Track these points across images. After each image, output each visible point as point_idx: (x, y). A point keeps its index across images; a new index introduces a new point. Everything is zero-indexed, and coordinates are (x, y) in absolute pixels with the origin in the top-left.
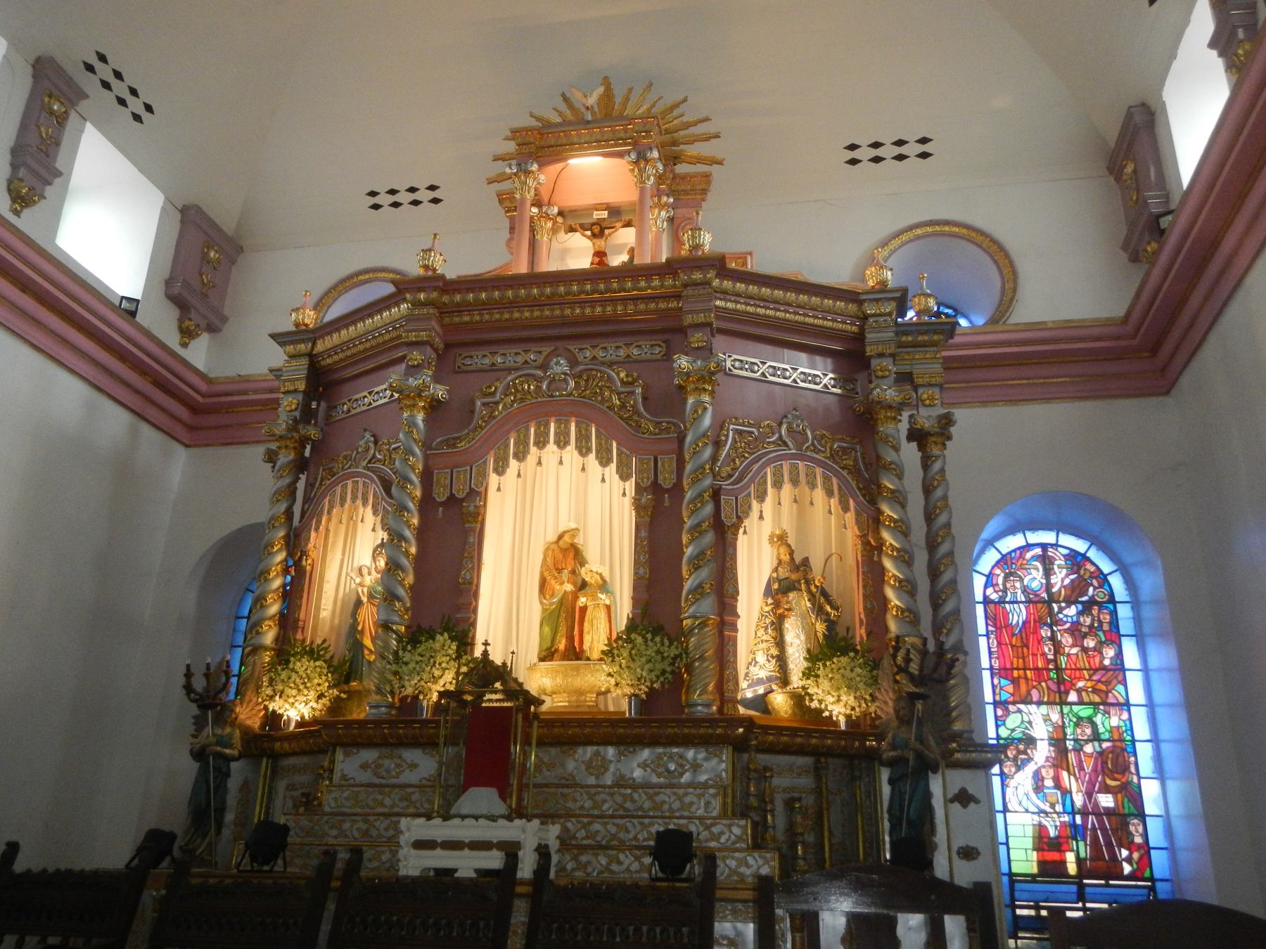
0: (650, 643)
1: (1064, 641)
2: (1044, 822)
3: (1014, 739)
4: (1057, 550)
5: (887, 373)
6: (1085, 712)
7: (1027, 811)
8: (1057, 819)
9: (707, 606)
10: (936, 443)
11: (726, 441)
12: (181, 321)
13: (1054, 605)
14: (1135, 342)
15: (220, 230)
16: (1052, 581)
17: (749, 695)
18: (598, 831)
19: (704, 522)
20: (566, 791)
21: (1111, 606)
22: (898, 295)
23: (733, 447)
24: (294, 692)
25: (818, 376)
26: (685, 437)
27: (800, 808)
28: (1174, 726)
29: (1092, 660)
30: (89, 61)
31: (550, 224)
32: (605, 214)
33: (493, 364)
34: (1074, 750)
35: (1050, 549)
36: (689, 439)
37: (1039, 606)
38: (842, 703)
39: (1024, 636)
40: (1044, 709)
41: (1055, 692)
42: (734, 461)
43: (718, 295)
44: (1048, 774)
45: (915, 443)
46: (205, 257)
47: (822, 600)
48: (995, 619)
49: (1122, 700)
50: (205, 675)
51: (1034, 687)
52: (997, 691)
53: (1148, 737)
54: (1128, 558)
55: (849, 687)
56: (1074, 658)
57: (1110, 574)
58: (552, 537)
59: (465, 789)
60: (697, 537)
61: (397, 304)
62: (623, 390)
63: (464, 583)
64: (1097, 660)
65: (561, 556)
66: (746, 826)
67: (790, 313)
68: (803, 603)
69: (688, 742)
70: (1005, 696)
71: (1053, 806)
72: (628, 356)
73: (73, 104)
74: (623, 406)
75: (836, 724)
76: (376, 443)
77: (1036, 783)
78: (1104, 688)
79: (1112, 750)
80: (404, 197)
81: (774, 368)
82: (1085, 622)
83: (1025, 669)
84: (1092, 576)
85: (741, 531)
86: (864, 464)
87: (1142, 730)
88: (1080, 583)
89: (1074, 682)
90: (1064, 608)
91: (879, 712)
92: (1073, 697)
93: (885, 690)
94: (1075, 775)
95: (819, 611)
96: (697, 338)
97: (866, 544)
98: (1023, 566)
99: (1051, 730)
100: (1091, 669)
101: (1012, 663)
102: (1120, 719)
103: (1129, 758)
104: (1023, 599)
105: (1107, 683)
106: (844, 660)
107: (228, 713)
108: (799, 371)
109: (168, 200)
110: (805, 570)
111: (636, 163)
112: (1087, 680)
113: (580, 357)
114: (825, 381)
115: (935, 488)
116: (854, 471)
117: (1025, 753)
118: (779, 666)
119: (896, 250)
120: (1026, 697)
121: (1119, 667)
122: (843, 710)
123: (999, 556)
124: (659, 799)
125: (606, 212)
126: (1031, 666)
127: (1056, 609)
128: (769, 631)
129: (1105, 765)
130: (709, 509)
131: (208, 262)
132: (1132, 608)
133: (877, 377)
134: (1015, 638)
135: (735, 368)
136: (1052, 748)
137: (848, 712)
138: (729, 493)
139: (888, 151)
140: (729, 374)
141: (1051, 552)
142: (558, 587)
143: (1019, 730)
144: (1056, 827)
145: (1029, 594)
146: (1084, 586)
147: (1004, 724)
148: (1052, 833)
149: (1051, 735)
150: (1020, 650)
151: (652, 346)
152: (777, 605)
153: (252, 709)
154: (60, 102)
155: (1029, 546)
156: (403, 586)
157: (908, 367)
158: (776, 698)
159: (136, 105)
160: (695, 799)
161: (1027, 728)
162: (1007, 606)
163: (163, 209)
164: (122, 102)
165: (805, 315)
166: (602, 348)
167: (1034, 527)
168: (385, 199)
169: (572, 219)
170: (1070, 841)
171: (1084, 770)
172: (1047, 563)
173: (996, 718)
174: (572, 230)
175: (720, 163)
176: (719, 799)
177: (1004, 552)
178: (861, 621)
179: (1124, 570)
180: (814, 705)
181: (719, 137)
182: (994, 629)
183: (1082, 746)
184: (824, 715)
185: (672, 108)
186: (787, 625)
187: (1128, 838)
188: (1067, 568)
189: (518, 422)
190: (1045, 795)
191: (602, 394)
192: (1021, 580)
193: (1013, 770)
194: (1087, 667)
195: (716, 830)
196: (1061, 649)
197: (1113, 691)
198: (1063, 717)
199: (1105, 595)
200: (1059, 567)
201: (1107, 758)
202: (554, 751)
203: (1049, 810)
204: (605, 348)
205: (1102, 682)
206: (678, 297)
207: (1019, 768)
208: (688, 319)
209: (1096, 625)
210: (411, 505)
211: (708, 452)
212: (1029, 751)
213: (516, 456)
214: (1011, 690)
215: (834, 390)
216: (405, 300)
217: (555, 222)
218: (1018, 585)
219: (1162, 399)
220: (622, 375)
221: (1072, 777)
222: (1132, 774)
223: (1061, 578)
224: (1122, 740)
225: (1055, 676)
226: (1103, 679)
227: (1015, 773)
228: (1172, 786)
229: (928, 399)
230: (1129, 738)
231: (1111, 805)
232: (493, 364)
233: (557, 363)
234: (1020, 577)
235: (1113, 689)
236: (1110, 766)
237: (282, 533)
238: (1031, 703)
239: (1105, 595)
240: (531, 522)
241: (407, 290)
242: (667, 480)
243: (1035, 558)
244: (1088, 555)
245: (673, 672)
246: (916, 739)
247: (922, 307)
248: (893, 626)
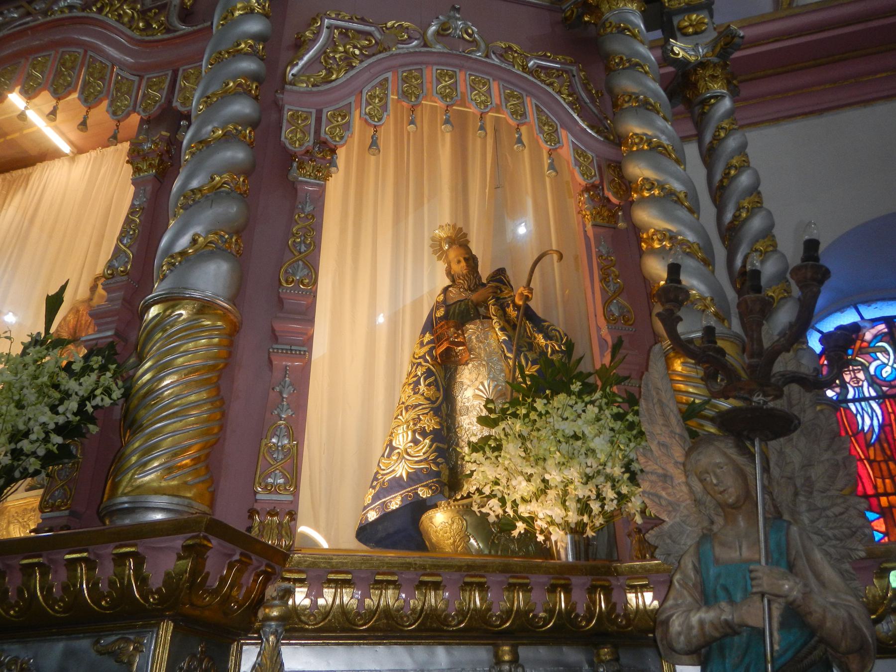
11: (314, 41)
17: (372, 516)
91: (652, 511)
93: (661, 445)
98: (864, 351)
101: (875, 487)
104: (873, 394)
118: (437, 450)
122: (557, 513)
128: (422, 387)
137: (573, 517)
150: (884, 466)
158: (431, 519)
184: (515, 533)
192: (866, 369)
218: (861, 375)
229: (691, 25)
234: (862, 364)
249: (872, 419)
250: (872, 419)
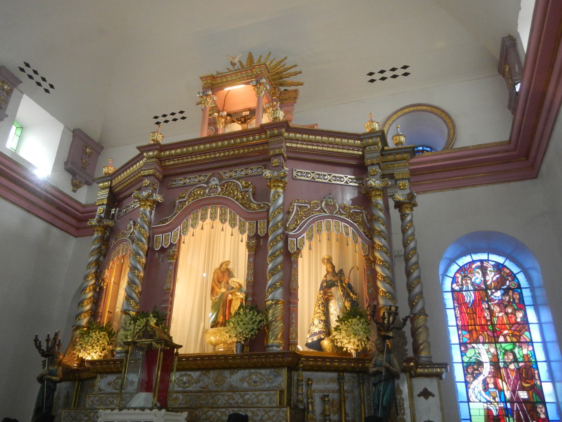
0: (248, 314)
1: (495, 310)
2: (491, 408)
3: (471, 363)
4: (488, 263)
5: (376, 173)
6: (509, 347)
7: (480, 401)
8: (497, 406)
9: (279, 294)
10: (407, 208)
11: (293, 211)
12: (72, 180)
13: (489, 291)
14: (516, 153)
15: (91, 139)
16: (487, 279)
17: (310, 341)
18: (212, 415)
19: (277, 251)
20: (199, 394)
21: (519, 290)
22: (380, 134)
23: (297, 214)
24: (90, 348)
25: (343, 177)
26: (270, 209)
27: (328, 401)
29: (510, 319)
30: (28, 68)
31: (223, 120)
32: (248, 113)
33: (185, 183)
34: (504, 367)
35: (485, 263)
36: (271, 210)
37: (481, 292)
38: (351, 343)
39: (473, 308)
40: (486, 346)
41: (492, 337)
42: (297, 221)
43: (287, 141)
44: (491, 381)
45: (398, 209)
46: (84, 152)
47: (349, 291)
48: (458, 300)
49: (528, 340)
50: (34, 340)
51: (481, 335)
52: (461, 337)
53: (544, 359)
55: (355, 335)
56: (501, 318)
57: (518, 273)
58: (217, 266)
59: (137, 393)
60: (273, 259)
61: (142, 159)
62: (242, 190)
63: (167, 289)
64: (513, 319)
65: (221, 275)
66: (287, 411)
67: (325, 147)
68: (339, 293)
69: (264, 367)
70: (465, 340)
71: (494, 398)
72: (247, 174)
73: (15, 86)
74: (243, 198)
75: (350, 354)
76: (134, 225)
77: (485, 386)
78: (518, 334)
79: (525, 367)
80: (169, 118)
81: (319, 174)
82: (505, 299)
83: (475, 325)
84: (508, 275)
85: (299, 256)
86: (368, 219)
87: (540, 355)
88: (501, 279)
89: (502, 331)
90: (494, 293)
91: (371, 348)
92: (501, 339)
93: (373, 335)
94: (505, 381)
95: (346, 296)
96: (275, 161)
97: (368, 260)
99: (491, 357)
100: (510, 324)
101: (468, 323)
102: (528, 350)
103: (534, 371)
105: (520, 331)
106: (354, 320)
107: (56, 359)
108: (332, 176)
109: (66, 127)
110: (341, 276)
111: (256, 86)
112: (509, 330)
113: (224, 177)
114: (346, 179)
115: (407, 230)
116: (361, 224)
117: (478, 370)
118: (325, 325)
119: (395, 120)
120: (477, 340)
121: (525, 323)
122: (353, 347)
123: (458, 268)
124: (247, 397)
125: (248, 112)
126: (478, 324)
127: (490, 293)
128: (321, 307)
129: (521, 376)
130: (280, 245)
131: (86, 154)
132: (531, 291)
133: (371, 175)
134: (469, 309)
135: (298, 176)
136: (492, 367)
137: (356, 348)
138: (292, 236)
139: (388, 74)
140: (294, 179)
141: (485, 264)
142: (218, 290)
143: (473, 358)
144: (497, 410)
145: (475, 286)
146: (504, 280)
147: (466, 355)
148: (495, 413)
149: (491, 360)
150: (472, 315)
151: (258, 168)
152: (325, 293)
153: (71, 357)
154: (9, 85)
155: (473, 262)
156: (135, 292)
157: (392, 171)
159: (45, 85)
160: (264, 397)
161: (478, 357)
162: (464, 293)
163: (63, 131)
164: (39, 84)
165: (333, 148)
166: (235, 171)
167: (476, 252)
168: (161, 119)
169: (233, 117)
170: (505, 417)
171: (510, 378)
172: (484, 270)
173: (461, 351)
174: (233, 122)
175: (302, 84)
176: (277, 397)
177: (461, 265)
178: (367, 300)
180: (339, 345)
181: (300, 73)
182: (457, 305)
183: (508, 366)
184: (344, 350)
186: (330, 304)
187: (537, 415)
188: (494, 272)
190: (490, 392)
191: (233, 193)
192: (471, 279)
193: (472, 379)
194: (508, 323)
195: (271, 414)
196: (494, 314)
197: (523, 335)
198: (497, 350)
199: (515, 284)
200: (490, 271)
201: (522, 370)
202: (198, 373)
203: (492, 400)
204: (236, 171)
205: (517, 331)
206: (267, 143)
207: (475, 378)
208: (271, 153)
209: (511, 300)
210: (141, 253)
211: (280, 217)
212: (480, 369)
213: (192, 226)
214: (468, 336)
215: (351, 184)
216: (144, 157)
217: (226, 119)
218: (469, 282)
219: (535, 180)
220: (244, 183)
221: (504, 383)
222: (537, 380)
223: (491, 277)
224: (531, 362)
225: (491, 329)
226: (518, 329)
227: (473, 381)
230: (533, 360)
231: (526, 397)
232: (185, 183)
233: (214, 180)
234: (470, 277)
235: (523, 334)
236: (524, 376)
237: (93, 271)
238: (479, 343)
239: (515, 284)
240: (212, 261)
241: (144, 151)
242: (261, 233)
243: (477, 267)
244: (505, 264)
245: (258, 329)
246: (386, 361)
247: (397, 141)
248: (381, 302)
249: (470, 298)
250: (470, 298)
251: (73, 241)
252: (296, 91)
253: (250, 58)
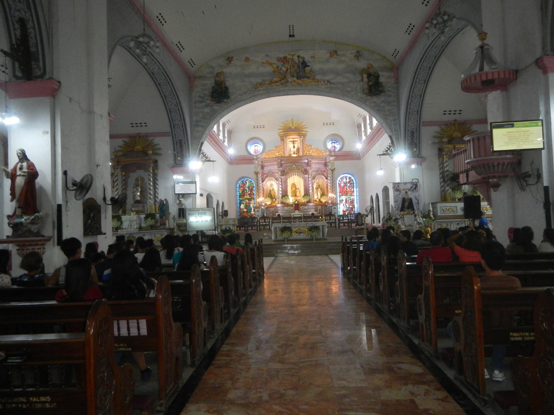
6: (349, 196)
28: (358, 198)
40: (345, 196)
44: (345, 204)
45: (331, 171)
54: (356, 178)
58: (292, 183)
87: (355, 198)
95: (321, 190)
121: (353, 191)
159: (229, 122)
167: (345, 174)
168: (256, 127)
174: (290, 141)
179: (355, 179)
185: (301, 123)
189: (291, 173)
223: (348, 180)
228: (358, 205)
251: (230, 166)
252: (306, 134)
253: (292, 120)
